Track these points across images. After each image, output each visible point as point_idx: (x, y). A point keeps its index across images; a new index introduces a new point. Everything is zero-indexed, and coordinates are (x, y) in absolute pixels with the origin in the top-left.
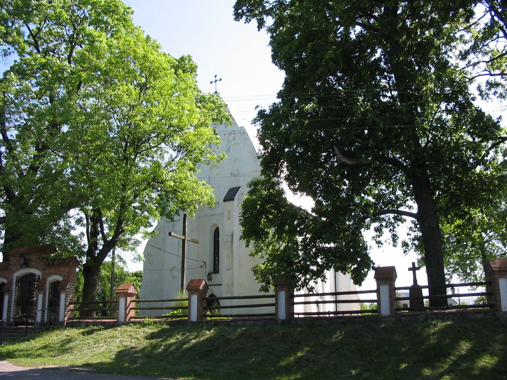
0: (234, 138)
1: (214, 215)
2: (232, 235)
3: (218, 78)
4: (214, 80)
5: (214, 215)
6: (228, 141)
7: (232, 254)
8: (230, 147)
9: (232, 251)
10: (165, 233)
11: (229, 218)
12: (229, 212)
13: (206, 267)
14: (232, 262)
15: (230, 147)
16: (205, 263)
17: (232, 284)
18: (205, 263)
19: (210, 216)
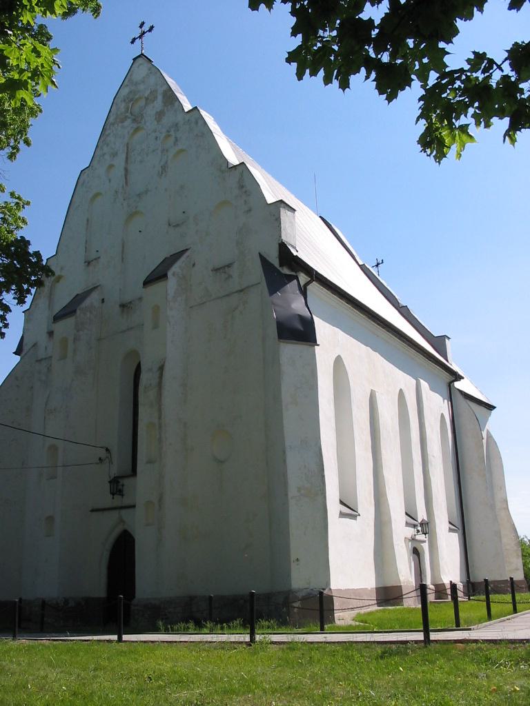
0: (176, 140)
1: (132, 328)
2: (161, 368)
3: (146, 28)
4: (138, 32)
5: (132, 328)
6: (163, 151)
7: (160, 418)
8: (166, 163)
9: (160, 410)
10: (32, 387)
11: (156, 326)
12: (156, 310)
13: (111, 462)
14: (160, 440)
15: (166, 163)
16: (107, 450)
17: (161, 500)
18: (107, 450)
19: (122, 332)
